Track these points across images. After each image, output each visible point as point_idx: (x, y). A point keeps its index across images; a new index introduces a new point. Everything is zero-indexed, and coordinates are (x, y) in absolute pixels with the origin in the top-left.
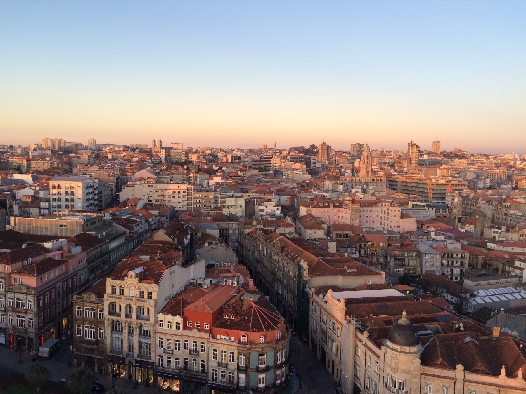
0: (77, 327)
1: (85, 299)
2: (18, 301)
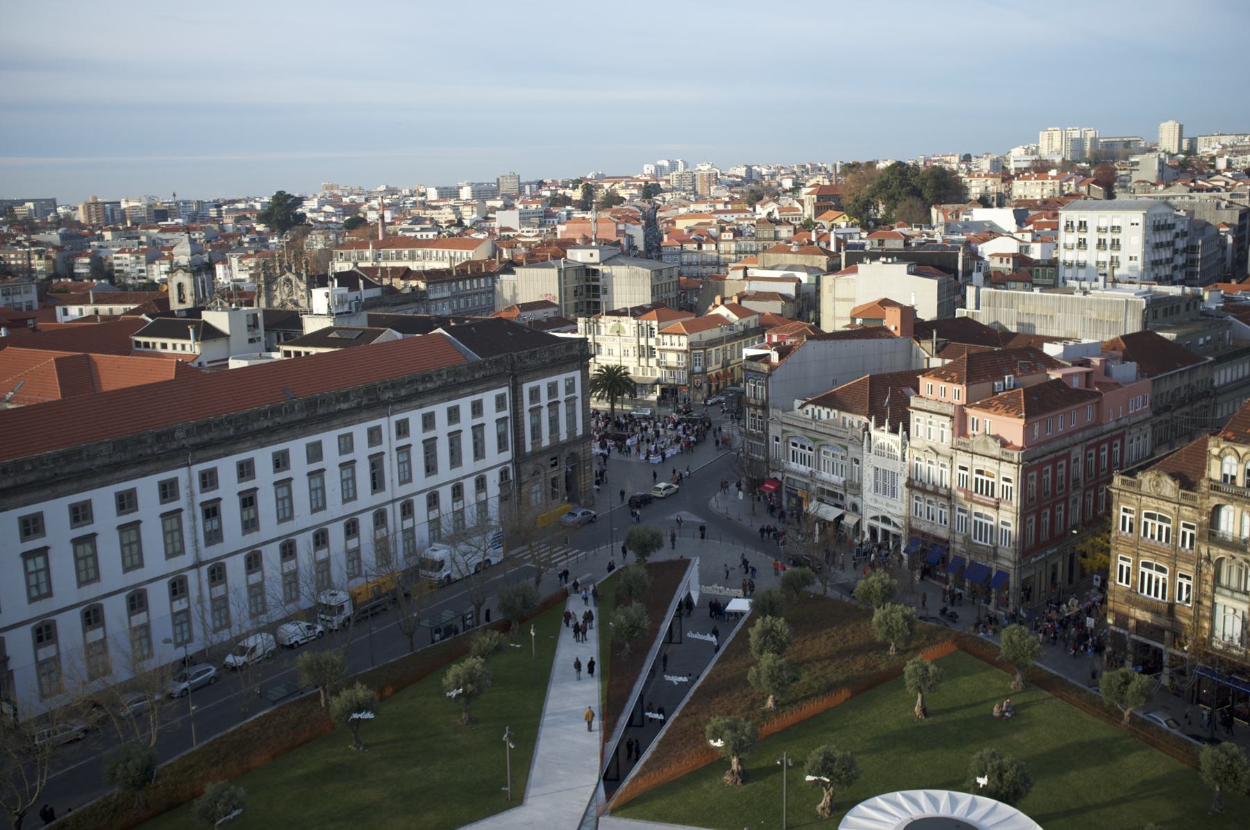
0: (1121, 562)
1: (1145, 487)
2: (980, 477)
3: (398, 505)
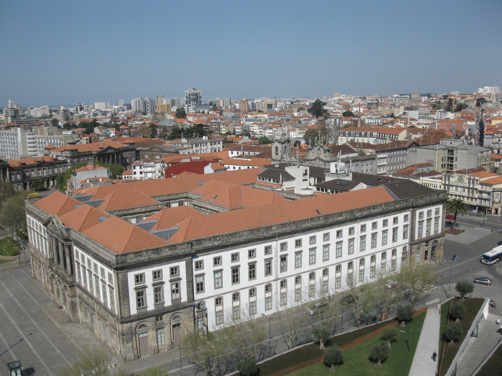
3: (358, 260)
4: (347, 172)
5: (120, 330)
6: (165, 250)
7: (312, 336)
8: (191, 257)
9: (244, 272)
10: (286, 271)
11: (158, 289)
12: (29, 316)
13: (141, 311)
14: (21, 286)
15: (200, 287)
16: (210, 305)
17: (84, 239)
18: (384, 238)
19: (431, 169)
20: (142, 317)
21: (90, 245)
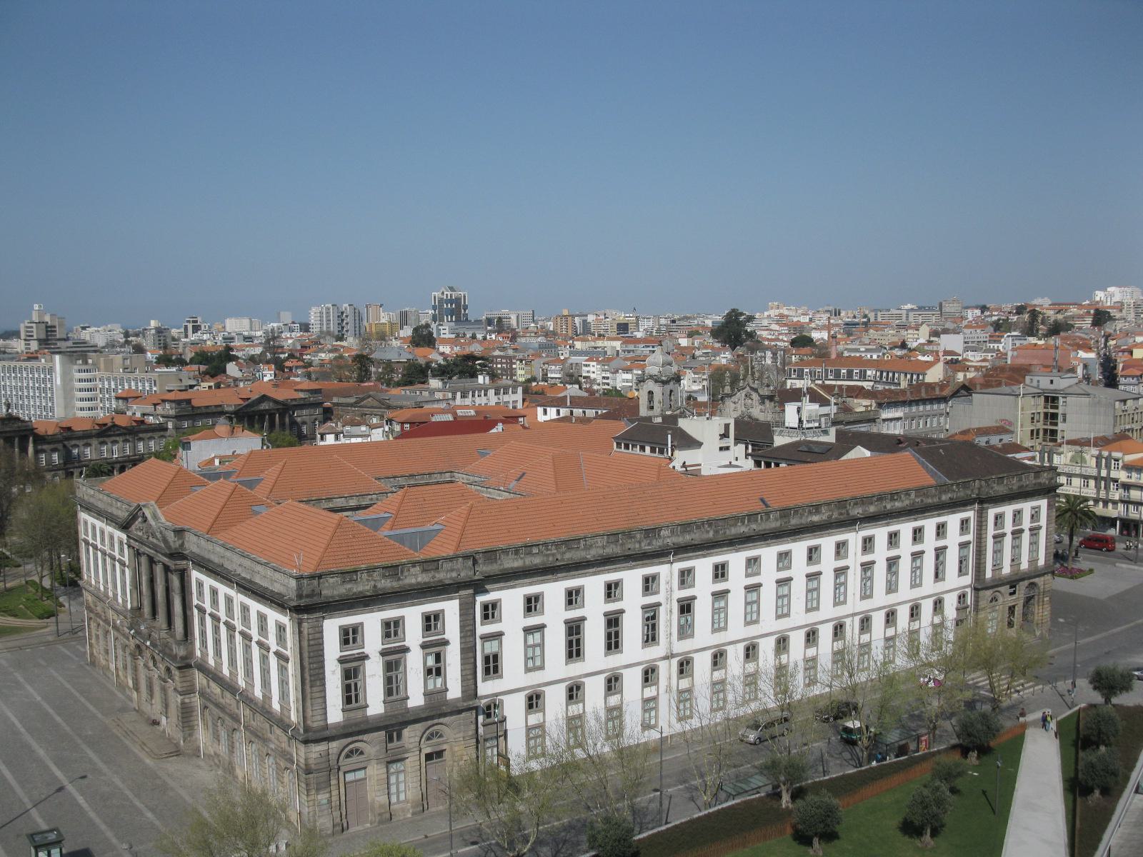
3: (857, 619)
4: (823, 426)
5: (302, 761)
6: (412, 570)
7: (758, 781)
8: (471, 591)
9: (594, 635)
10: (692, 636)
11: (394, 661)
12: (79, 741)
13: (352, 714)
14: (60, 679)
15: (491, 665)
16: (514, 710)
17: (219, 549)
18: (916, 570)
19: (1007, 439)
20: (355, 729)
21: (234, 563)
